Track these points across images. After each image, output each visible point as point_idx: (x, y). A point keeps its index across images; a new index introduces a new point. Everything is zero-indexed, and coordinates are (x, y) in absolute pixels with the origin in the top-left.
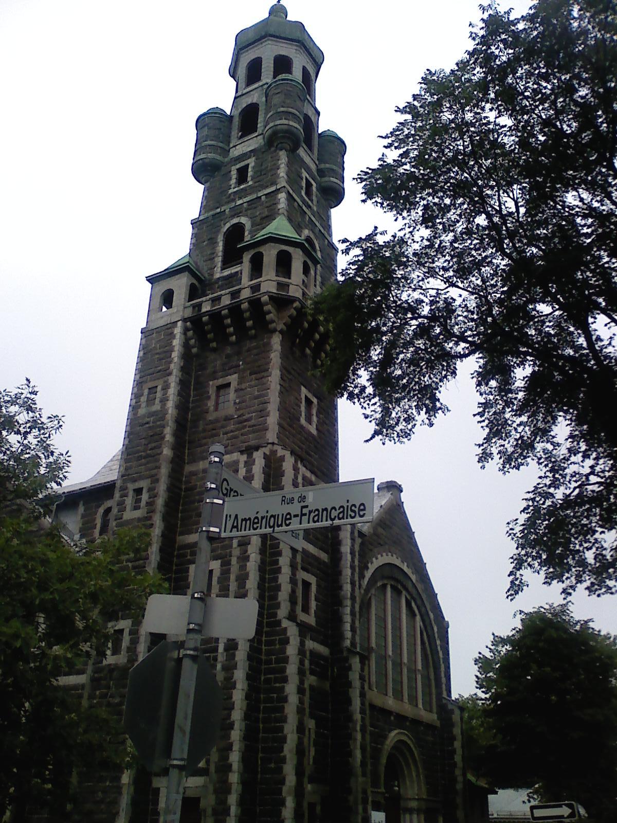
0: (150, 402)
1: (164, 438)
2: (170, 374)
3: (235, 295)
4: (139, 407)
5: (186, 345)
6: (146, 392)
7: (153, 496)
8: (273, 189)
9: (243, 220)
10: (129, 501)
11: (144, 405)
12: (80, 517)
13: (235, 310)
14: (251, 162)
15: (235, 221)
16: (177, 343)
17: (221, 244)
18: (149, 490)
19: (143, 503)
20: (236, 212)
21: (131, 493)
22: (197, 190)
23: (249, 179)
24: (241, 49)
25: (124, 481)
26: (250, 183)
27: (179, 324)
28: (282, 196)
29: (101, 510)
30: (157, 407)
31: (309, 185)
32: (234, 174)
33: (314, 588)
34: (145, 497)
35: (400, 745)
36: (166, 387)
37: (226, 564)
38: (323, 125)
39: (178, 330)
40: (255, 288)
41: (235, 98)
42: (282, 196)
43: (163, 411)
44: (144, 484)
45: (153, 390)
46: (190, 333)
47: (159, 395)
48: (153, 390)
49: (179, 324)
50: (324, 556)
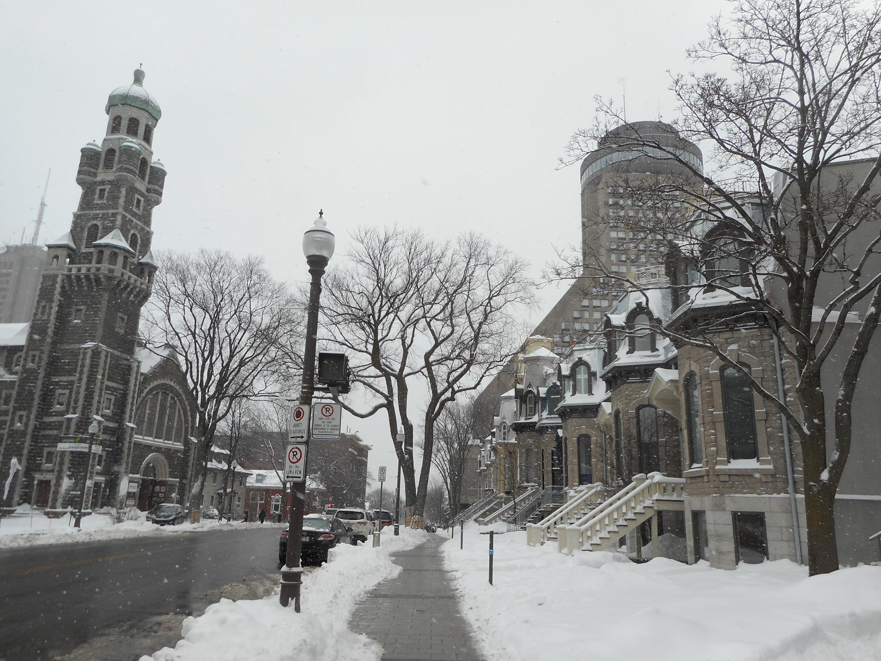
0: (43, 313)
1: (47, 333)
2: (53, 302)
3: (89, 270)
4: (37, 314)
5: (63, 287)
6: (41, 308)
7: (40, 359)
8: (114, 211)
9: (99, 223)
10: (30, 359)
11: (39, 314)
12: (4, 357)
13: (87, 277)
14: (107, 187)
15: (94, 222)
16: (58, 286)
17: (86, 233)
18: (40, 357)
19: (36, 362)
20: (96, 217)
21: (30, 356)
22: (79, 191)
23: (105, 198)
24: (112, 105)
25: (28, 350)
26: (105, 201)
27: (60, 276)
28: (119, 218)
29: (16, 357)
30: (45, 317)
31: (139, 201)
32: (98, 191)
33: (113, 401)
34: (37, 359)
35: (154, 459)
36: (51, 308)
37: (71, 392)
38: (154, 159)
39: (59, 280)
40: (98, 269)
41: (104, 140)
42: (119, 218)
43: (48, 321)
44: (37, 353)
45: (44, 307)
46: (65, 281)
47: (47, 311)
48: (44, 307)
49: (60, 276)
50: (121, 387)
